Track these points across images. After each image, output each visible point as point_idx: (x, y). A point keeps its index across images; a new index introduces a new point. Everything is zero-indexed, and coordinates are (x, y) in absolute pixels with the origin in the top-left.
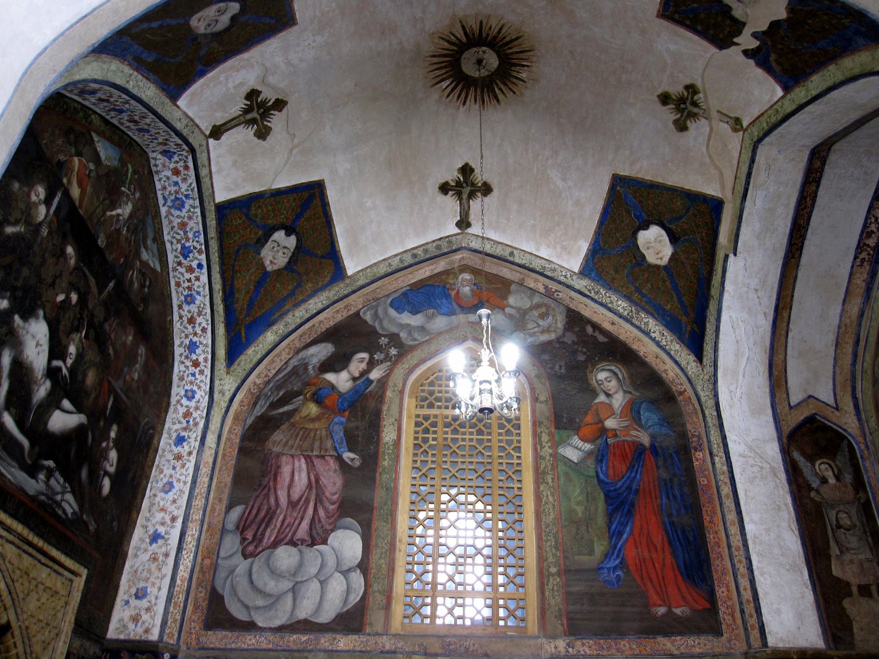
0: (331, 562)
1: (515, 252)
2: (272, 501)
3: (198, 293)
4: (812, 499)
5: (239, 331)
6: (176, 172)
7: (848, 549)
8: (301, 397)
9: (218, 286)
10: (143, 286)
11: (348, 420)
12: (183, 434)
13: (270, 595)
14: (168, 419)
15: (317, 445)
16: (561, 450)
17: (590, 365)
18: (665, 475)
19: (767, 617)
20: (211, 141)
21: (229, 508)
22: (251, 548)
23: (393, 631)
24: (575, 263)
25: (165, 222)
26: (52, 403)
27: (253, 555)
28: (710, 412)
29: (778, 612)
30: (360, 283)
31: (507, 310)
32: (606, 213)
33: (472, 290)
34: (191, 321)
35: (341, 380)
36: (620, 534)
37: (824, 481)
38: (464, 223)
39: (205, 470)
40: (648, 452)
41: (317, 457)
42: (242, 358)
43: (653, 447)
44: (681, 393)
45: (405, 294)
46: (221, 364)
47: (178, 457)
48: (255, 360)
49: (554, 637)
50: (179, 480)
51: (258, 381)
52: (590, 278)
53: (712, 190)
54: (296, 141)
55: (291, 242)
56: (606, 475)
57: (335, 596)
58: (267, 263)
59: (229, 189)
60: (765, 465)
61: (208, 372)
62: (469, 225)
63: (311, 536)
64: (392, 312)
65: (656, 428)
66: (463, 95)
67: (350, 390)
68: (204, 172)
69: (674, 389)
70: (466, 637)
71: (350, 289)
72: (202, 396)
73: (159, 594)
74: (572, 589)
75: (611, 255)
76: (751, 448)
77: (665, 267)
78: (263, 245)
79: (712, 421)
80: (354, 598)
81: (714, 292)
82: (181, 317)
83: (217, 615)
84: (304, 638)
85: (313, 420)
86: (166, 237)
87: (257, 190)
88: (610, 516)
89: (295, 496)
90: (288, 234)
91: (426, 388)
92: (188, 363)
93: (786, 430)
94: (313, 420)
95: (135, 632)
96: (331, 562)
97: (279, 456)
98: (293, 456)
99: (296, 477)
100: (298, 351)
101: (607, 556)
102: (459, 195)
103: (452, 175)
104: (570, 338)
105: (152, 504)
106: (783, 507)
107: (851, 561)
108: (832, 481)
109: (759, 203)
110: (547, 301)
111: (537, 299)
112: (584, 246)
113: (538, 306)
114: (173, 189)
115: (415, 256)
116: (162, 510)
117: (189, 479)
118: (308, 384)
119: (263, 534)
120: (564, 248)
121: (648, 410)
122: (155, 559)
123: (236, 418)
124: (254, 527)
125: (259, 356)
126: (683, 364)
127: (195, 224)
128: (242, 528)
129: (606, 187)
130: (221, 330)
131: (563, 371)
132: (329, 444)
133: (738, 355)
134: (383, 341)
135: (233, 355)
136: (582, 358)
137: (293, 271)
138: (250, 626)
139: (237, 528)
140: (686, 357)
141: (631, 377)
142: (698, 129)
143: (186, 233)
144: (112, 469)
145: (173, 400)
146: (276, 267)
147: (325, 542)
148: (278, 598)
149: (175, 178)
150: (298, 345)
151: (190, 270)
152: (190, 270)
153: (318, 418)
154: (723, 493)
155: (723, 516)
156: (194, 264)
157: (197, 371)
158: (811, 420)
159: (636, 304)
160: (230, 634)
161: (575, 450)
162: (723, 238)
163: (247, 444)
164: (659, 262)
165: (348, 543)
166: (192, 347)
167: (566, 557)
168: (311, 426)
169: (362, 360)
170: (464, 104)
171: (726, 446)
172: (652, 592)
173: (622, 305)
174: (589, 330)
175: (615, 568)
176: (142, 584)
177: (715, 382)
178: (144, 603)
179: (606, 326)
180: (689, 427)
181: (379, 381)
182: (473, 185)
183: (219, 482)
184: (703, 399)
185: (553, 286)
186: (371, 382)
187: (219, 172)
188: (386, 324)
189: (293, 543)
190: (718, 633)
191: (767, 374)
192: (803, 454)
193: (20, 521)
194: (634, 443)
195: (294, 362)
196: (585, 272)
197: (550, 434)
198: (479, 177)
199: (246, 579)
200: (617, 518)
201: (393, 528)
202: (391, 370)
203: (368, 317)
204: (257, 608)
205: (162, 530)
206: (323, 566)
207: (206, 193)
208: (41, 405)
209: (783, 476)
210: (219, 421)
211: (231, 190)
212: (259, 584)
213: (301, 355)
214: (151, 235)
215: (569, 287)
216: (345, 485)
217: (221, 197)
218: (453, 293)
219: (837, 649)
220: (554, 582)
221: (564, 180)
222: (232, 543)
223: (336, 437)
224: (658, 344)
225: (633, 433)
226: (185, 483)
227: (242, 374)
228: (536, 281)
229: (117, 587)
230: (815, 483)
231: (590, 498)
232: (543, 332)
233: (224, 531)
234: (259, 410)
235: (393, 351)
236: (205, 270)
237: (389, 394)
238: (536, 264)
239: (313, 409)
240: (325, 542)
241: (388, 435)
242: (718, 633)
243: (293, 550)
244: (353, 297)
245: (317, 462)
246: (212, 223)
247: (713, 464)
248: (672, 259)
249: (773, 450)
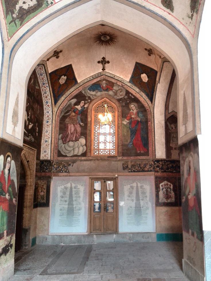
0: (80, 144)
1: (115, 76)
2: (67, 133)
3: (47, 92)
4: (169, 132)
5: (56, 98)
6: (40, 69)
7: (174, 141)
8: (71, 111)
9: (51, 90)
10: (37, 94)
11: (81, 116)
12: (48, 121)
13: (69, 151)
14: (44, 117)
15: (75, 122)
16: (123, 122)
17: (130, 103)
18: (142, 127)
19: (156, 153)
20: (47, 62)
21: (59, 135)
22: (64, 142)
23: (92, 156)
24: (128, 80)
25: (39, 78)
26: (29, 124)
27: (65, 143)
28: (152, 114)
29: (158, 153)
30: (81, 84)
31: (113, 90)
32: (134, 69)
33: (106, 86)
34: (46, 97)
35: (79, 107)
36: (133, 138)
37: (172, 128)
39: (54, 128)
40: (140, 122)
41: (75, 124)
42: (58, 103)
43: (141, 121)
44: (148, 110)
45: (91, 86)
46: (53, 105)
47: (48, 125)
48: (60, 103)
49: (120, 157)
50: (49, 130)
51: (61, 108)
52: (131, 83)
53: (156, 69)
54: (65, 57)
55: (66, 77)
56: (131, 127)
57: (81, 150)
58: (61, 83)
59: (51, 70)
60: (161, 125)
61: (51, 107)
62: (105, 70)
63: (76, 140)
64: (89, 91)
65: (142, 117)
66: (102, 44)
67: (81, 110)
68: (46, 68)
69: (146, 108)
70: (104, 157)
71: (79, 86)
72: (50, 112)
73: (49, 151)
74: (123, 148)
75: (135, 79)
76: (159, 122)
77: (146, 83)
78: (59, 79)
79: (152, 116)
80: (85, 151)
81: (155, 90)
82: (44, 96)
83: (60, 154)
84: (76, 158)
85: (74, 116)
86: (39, 81)
87: (57, 68)
88: (131, 135)
89: (72, 132)
90: (65, 76)
91: (96, 109)
92: (47, 106)
93: (167, 118)
94: (74, 116)
95: (45, 158)
96: (80, 144)
97: (68, 124)
98: (70, 124)
99: (72, 128)
100: (69, 101)
101: (130, 142)
102: (102, 63)
103: (100, 59)
104: (126, 97)
105: (44, 135)
106: (163, 134)
107: (174, 144)
108: (174, 128)
109: (164, 73)
110: (122, 88)
111: (120, 88)
112: (130, 76)
113: (120, 89)
114: (40, 72)
115: (93, 77)
116: (46, 136)
117: (51, 130)
118: (72, 108)
119: (67, 139)
120: (126, 76)
121: (141, 113)
122: (47, 145)
123: (58, 116)
124: (65, 138)
125: (61, 103)
126: (149, 104)
127: (45, 78)
128: (62, 138)
129: (134, 64)
130: (53, 98)
131: (124, 105)
132: (77, 121)
133: (159, 103)
134: (87, 98)
135: (55, 103)
136: (128, 102)
137: (66, 84)
138: (66, 156)
139: (61, 139)
140: (149, 102)
141: (138, 106)
142: (153, 57)
143: (43, 80)
144: (37, 131)
145: (45, 113)
146: (62, 83)
147: (78, 141)
148: (70, 151)
149: (40, 70)
150: (69, 99)
151: (45, 87)
152: (45, 87)
153: (75, 116)
154: (152, 131)
155: (152, 135)
156: (46, 86)
157: (49, 107)
158: (172, 116)
159: (140, 90)
160: (62, 158)
161: (125, 122)
162: (157, 79)
163: (61, 122)
164: (145, 81)
165: (83, 141)
166: (47, 102)
167: (122, 143)
168: (73, 118)
169: (83, 103)
170: (102, 45)
171: (154, 122)
172: (137, 149)
173: (137, 90)
174: (130, 95)
175: (131, 145)
176: (45, 150)
177: (154, 108)
178: (46, 153)
179: (134, 94)
180: (148, 117)
181: (87, 107)
182: (105, 61)
183: (56, 130)
184: (152, 112)
185: (123, 84)
186: (85, 108)
187: (49, 67)
188: (87, 94)
189: (72, 141)
190: (148, 155)
191: (164, 107)
192: (169, 123)
193: (27, 145)
194: (137, 120)
195: (68, 103)
196: (130, 82)
197: (121, 119)
198: (107, 60)
199: (64, 148)
200: (133, 135)
201: (91, 138)
202: (89, 105)
203: (83, 92)
204: (67, 153)
205: (47, 140)
206: (78, 145)
207: (47, 72)
208: (28, 125)
209: (164, 128)
210: (55, 117)
211: (52, 70)
212: (67, 149)
213: (70, 101)
214: (36, 82)
215: (127, 85)
216: (81, 130)
217: (50, 72)
218: (102, 86)
219: (168, 159)
220: (120, 147)
221: (125, 61)
222: (60, 142)
223: (79, 120)
224: (144, 99)
225: (137, 118)
226: (50, 131)
227: (58, 107)
228: (120, 83)
229: (41, 151)
230: (171, 129)
231: (128, 131)
232: (121, 96)
233: (59, 139)
234: (62, 114)
235: (89, 101)
236: (48, 87)
237: (89, 110)
238: (120, 79)
239: (74, 114)
240: (78, 141)
241: (89, 120)
242: (148, 155)
243: (73, 142)
244: (80, 87)
245: (75, 125)
246: (49, 78)
247: (152, 125)
248: (148, 81)
249: (163, 123)
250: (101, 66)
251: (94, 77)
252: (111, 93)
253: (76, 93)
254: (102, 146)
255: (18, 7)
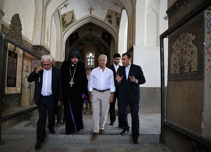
35: (80, 48)
38: (90, 32)
112: (101, 36)
173: (104, 41)
250: (89, 31)
251: (86, 36)
252: (93, 42)
253: (79, 42)
254: (89, 64)
255: (66, 24)
